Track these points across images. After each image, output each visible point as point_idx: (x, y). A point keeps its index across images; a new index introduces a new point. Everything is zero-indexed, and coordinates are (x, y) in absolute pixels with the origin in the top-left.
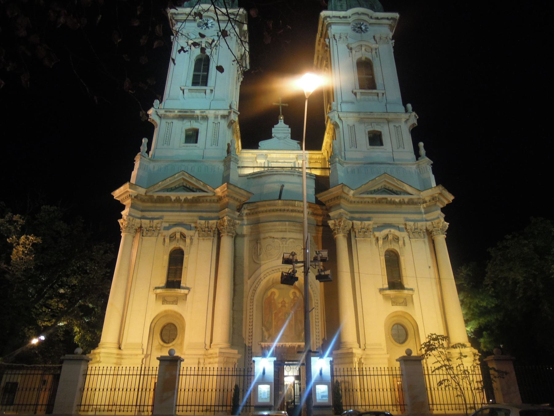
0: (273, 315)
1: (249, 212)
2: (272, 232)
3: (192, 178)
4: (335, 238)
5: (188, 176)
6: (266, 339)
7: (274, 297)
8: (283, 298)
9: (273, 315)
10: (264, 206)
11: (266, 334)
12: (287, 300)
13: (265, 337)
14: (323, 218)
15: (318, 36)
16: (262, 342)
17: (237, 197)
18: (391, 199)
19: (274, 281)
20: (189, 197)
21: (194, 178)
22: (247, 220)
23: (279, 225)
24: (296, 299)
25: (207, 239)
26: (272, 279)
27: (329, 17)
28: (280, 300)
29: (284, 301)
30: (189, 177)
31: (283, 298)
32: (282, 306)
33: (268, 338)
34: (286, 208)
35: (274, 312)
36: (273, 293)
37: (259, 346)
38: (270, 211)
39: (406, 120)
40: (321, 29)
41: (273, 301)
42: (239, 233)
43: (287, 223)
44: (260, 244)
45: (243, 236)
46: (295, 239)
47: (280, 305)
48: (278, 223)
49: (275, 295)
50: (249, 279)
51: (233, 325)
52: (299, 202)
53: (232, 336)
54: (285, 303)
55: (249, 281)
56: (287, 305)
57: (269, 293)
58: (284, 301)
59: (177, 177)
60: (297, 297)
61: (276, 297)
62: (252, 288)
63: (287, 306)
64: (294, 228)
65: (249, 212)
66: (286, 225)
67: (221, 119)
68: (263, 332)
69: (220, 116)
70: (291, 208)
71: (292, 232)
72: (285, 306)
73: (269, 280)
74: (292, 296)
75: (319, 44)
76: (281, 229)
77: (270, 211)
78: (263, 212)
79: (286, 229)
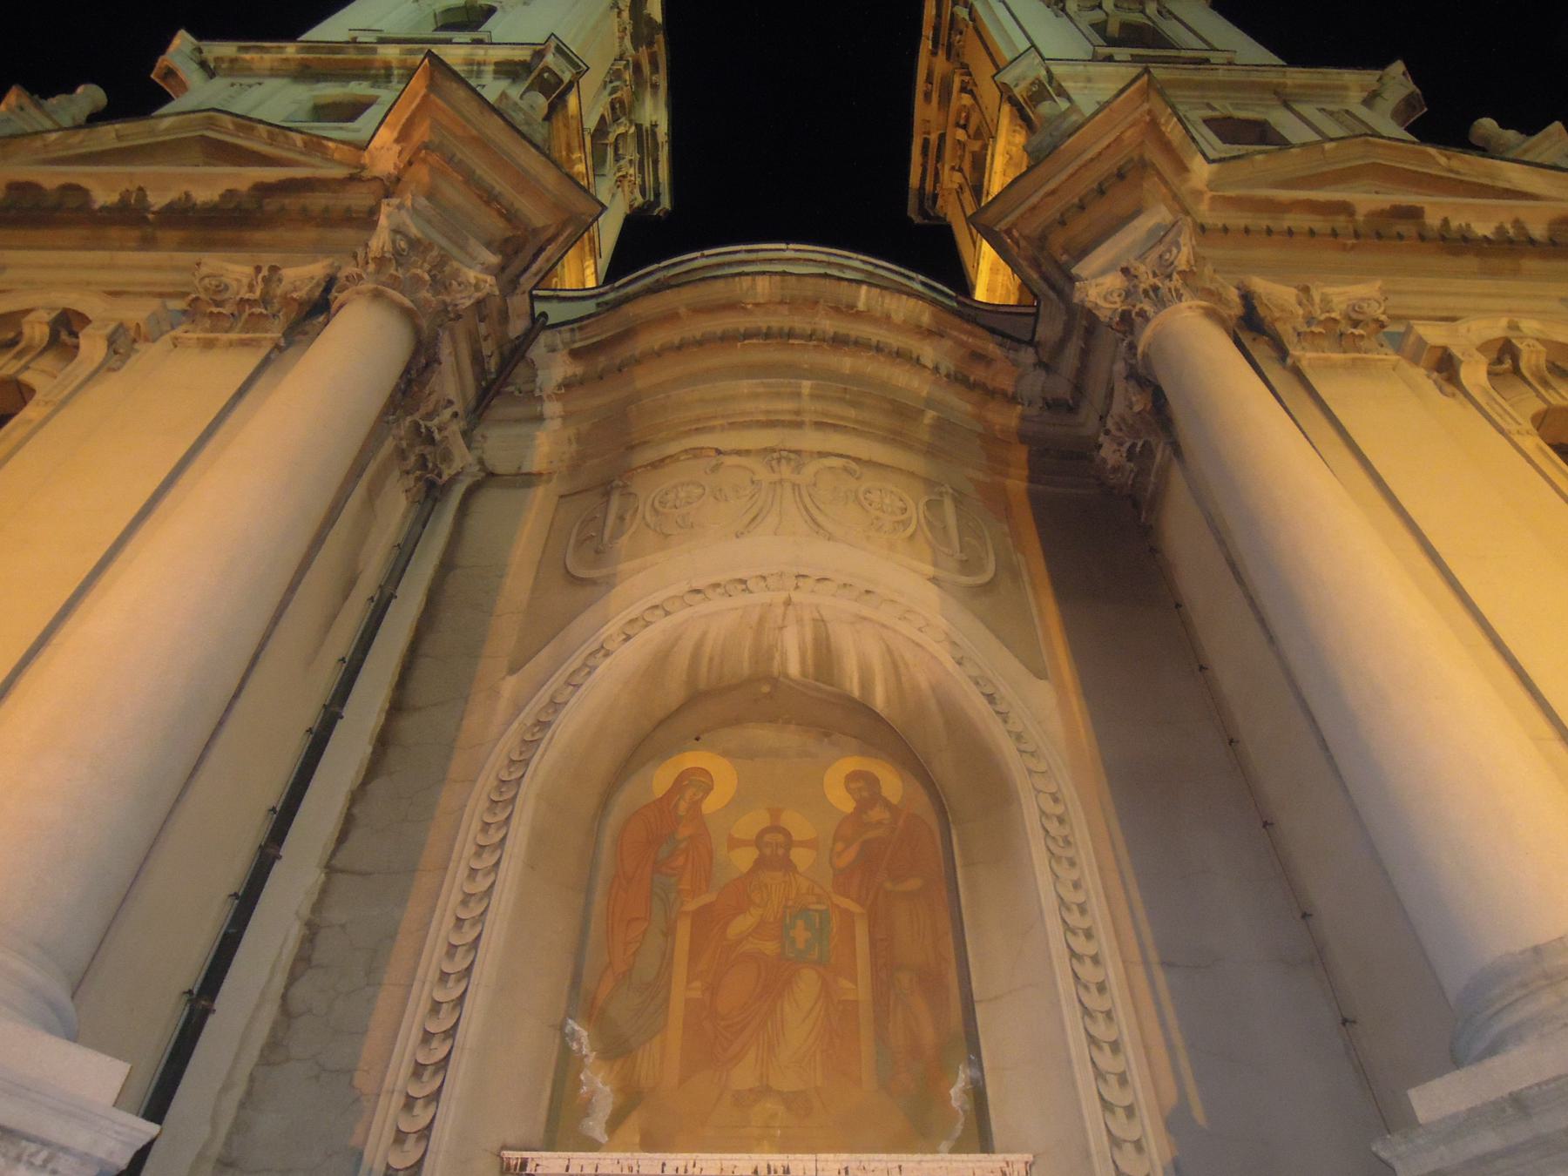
1: (575, 369)
2: (712, 429)
3: (252, 129)
4: (1145, 355)
5: (231, 126)
6: (596, 1126)
7: (696, 805)
8: (775, 813)
9: (683, 931)
10: (671, 317)
11: (599, 1084)
12: (799, 824)
13: (586, 1109)
14: (1023, 418)
15: (926, 45)
16: (550, 1145)
17: (500, 184)
18: (1446, 222)
19: (704, 669)
20: (204, 195)
21: (261, 126)
22: (566, 417)
23: (755, 396)
24: (877, 814)
25: (231, 344)
26: (681, 660)
28: (751, 823)
29: (775, 828)
30: (239, 127)
31: (775, 813)
32: (760, 864)
34: (799, 323)
35: (692, 905)
36: (699, 781)
38: (702, 343)
39: (1365, 94)
40: (934, 12)
41: (684, 832)
42: (502, 465)
43: (806, 386)
44: (627, 493)
45: (527, 480)
46: (857, 460)
47: (744, 859)
48: (746, 385)
49: (708, 789)
50: (512, 671)
51: (293, 978)
52: (876, 291)
53: (252, 1079)
54: (789, 843)
55: (510, 686)
56: (801, 858)
57: (661, 778)
58: (775, 828)
59: (167, 131)
60: (887, 805)
61: (711, 804)
62: (527, 716)
63: (801, 868)
64: (852, 413)
65: (575, 369)
66: (799, 395)
67: (495, 78)
68: (567, 1065)
69: (491, 68)
70: (828, 325)
71: (834, 427)
72: (788, 866)
73: (661, 659)
74: (847, 805)
75: (927, 96)
76: (768, 412)
77: (702, 343)
78: (659, 354)
79: (798, 413)
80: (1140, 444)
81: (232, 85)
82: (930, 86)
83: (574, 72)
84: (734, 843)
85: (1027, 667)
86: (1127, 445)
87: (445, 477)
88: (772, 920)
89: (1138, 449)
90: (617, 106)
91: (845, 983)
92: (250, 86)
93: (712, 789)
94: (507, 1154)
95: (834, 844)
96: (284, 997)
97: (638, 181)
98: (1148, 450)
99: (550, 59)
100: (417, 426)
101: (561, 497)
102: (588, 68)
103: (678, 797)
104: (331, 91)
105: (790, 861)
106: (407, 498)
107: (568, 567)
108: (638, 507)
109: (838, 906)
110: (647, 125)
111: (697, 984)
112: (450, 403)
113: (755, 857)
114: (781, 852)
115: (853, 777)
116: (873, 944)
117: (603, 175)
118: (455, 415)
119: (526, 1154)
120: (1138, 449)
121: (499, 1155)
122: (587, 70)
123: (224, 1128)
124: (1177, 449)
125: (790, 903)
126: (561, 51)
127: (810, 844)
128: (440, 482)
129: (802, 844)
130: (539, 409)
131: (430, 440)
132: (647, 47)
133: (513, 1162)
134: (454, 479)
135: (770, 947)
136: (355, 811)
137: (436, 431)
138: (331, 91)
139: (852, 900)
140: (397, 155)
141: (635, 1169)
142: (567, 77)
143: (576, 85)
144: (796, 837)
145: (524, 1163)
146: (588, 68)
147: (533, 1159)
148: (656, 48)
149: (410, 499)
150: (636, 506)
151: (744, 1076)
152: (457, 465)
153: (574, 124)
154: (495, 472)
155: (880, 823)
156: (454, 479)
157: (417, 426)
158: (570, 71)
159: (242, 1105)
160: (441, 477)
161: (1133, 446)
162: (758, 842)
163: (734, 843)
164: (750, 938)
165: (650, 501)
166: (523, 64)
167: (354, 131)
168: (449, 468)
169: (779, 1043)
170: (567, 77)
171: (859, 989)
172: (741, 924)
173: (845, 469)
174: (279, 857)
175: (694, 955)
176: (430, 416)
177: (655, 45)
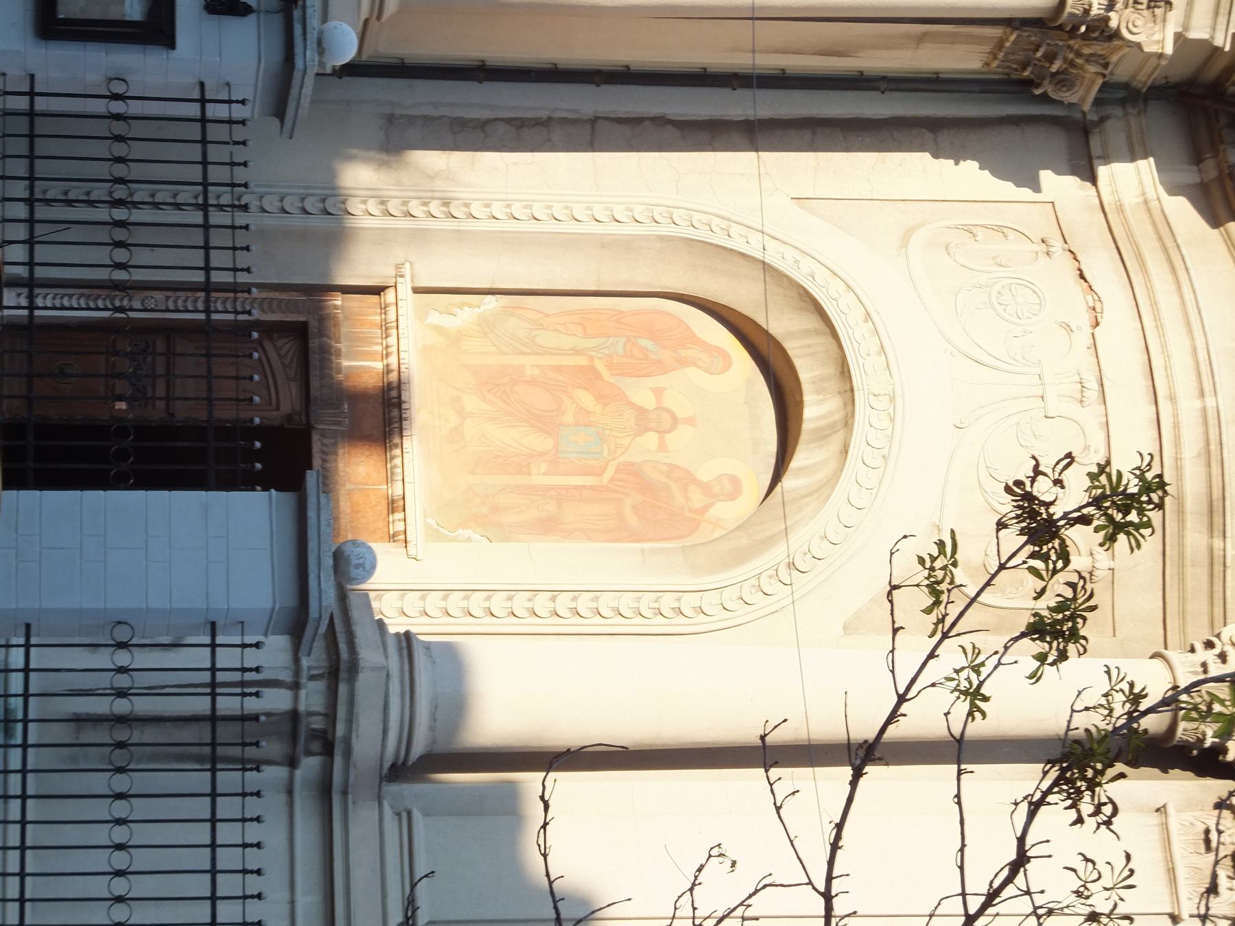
0: (582, 361)
6: (434, 318)
7: (693, 363)
8: (691, 421)
12: (679, 439)
24: (697, 499)
31: (691, 421)
32: (641, 411)
33: (439, 330)
35: (600, 366)
37: (393, 272)
51: (508, 121)
53: (441, 117)
54: (661, 432)
56: (651, 439)
58: (675, 421)
84: (658, 392)
88: (592, 419)
91: (544, 467)
93: (711, 374)
94: (407, 265)
95: (665, 464)
96: (496, 119)
103: (700, 349)
105: (645, 432)
109: (607, 464)
111: (536, 372)
113: (647, 408)
114: (653, 425)
115: (735, 482)
116: (577, 488)
119: (408, 277)
121: (406, 261)
123: (411, 112)
125: (607, 432)
127: (662, 447)
129: (662, 441)
130: (1208, 155)
133: (403, 270)
134: (1045, 99)
135: (569, 418)
136: (647, 123)
139: (613, 475)
141: (403, 336)
144: (668, 436)
145: (402, 276)
147: (405, 280)
151: (471, 402)
154: (1090, 136)
155: (688, 499)
159: (425, 117)
162: (659, 408)
163: (658, 392)
164: (575, 405)
169: (495, 424)
171: (538, 479)
172: (586, 399)
174: (598, 86)
175: (559, 369)
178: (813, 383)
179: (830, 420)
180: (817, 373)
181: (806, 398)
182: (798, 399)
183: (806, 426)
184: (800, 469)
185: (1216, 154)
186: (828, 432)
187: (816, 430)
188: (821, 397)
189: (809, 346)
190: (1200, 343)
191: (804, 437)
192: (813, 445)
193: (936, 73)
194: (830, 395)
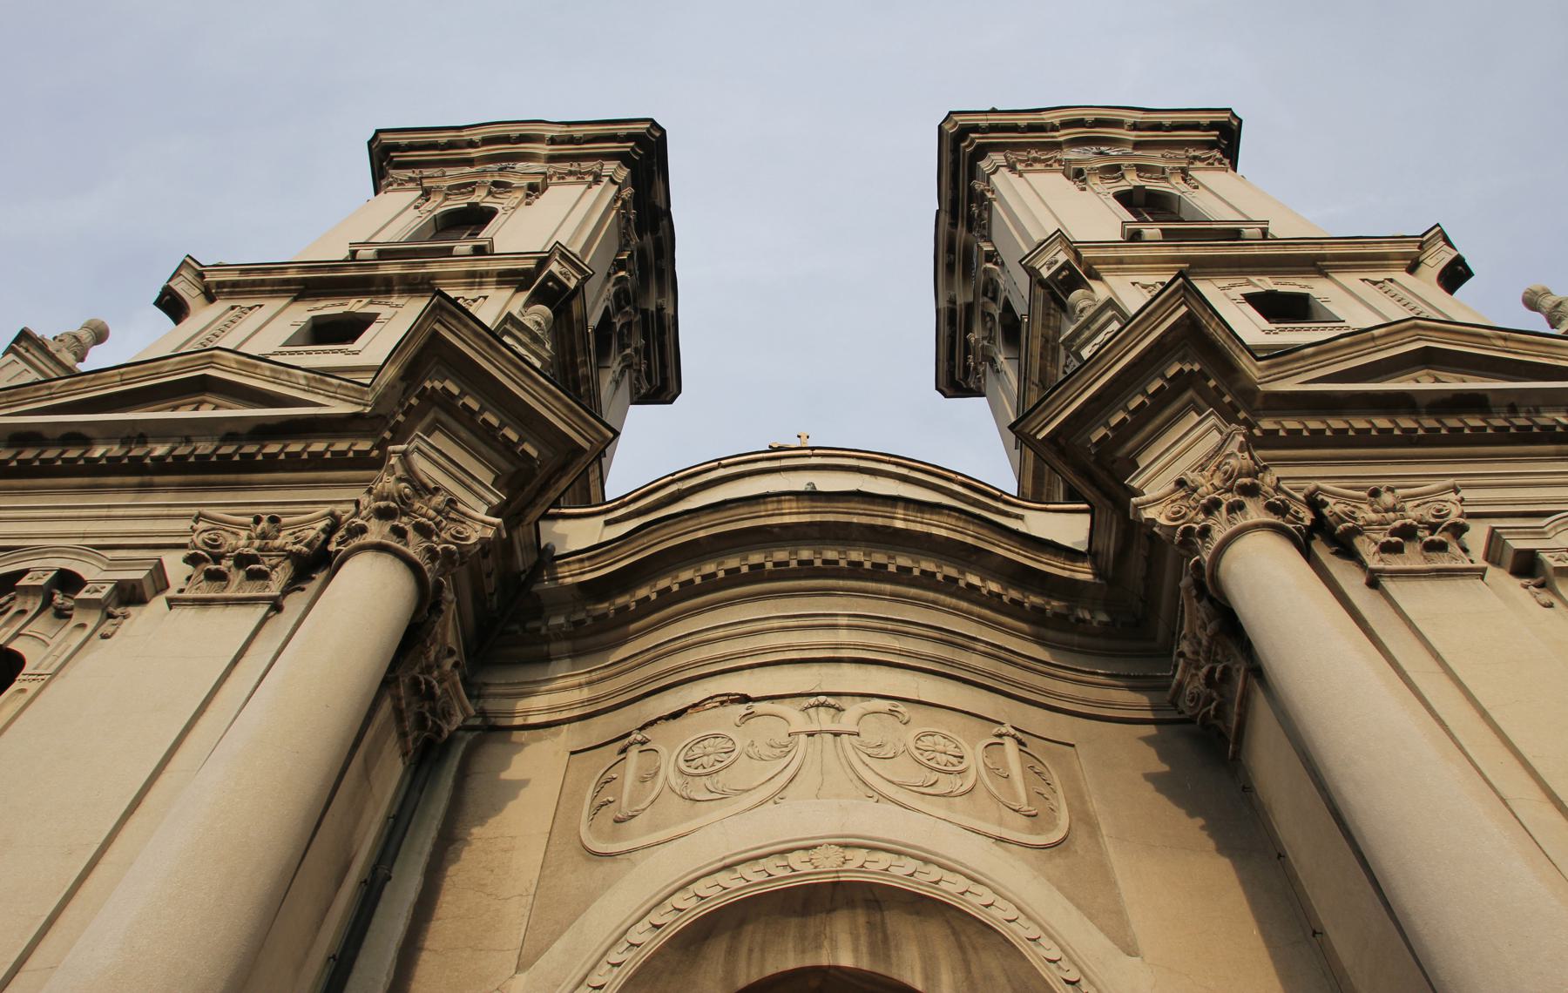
27: (975, 128)
80: (1219, 668)
81: (233, 308)
82: (952, 256)
83: (580, 277)
85: (1113, 939)
86: (1205, 670)
87: (445, 735)
89: (1217, 675)
90: (622, 296)
92: (251, 309)
97: (643, 368)
98: (1227, 674)
99: (554, 267)
100: (415, 683)
101: (573, 753)
102: (594, 273)
104: (330, 308)
106: (404, 763)
107: (583, 840)
108: (659, 766)
110: (653, 308)
112: (451, 653)
117: (609, 367)
118: (456, 665)
120: (1217, 675)
122: (592, 275)
124: (1257, 672)
126: (565, 257)
128: (440, 741)
131: (430, 695)
132: (651, 234)
137: (437, 685)
138: (330, 308)
140: (401, 392)
142: (572, 284)
143: (581, 289)
146: (594, 273)
148: (661, 233)
149: (407, 763)
150: (658, 764)
152: (458, 719)
153: (577, 327)
156: (452, 738)
157: (415, 683)
158: (575, 277)
160: (440, 735)
161: (1212, 671)
165: (674, 758)
166: (525, 272)
167: (356, 353)
168: (449, 723)
170: (572, 284)
173: (891, 712)
176: (428, 669)
177: (661, 231)
178: (803, 952)
179: (862, 931)
180: (790, 945)
181: (825, 960)
182: (814, 983)
183: (865, 964)
184: (927, 977)
185: (547, 640)
186: (880, 936)
187: (873, 953)
188: (826, 943)
189: (751, 950)
190: (776, 624)
191: (880, 969)
192: (894, 960)
193: (388, 818)
194: (827, 928)
